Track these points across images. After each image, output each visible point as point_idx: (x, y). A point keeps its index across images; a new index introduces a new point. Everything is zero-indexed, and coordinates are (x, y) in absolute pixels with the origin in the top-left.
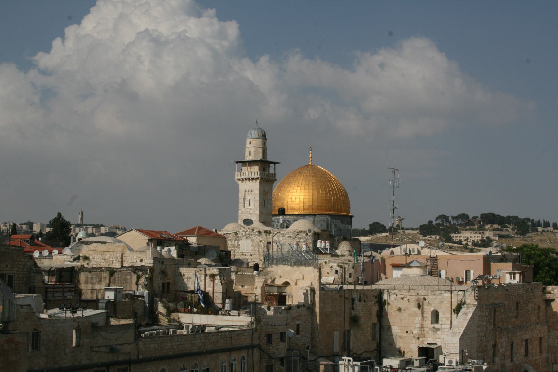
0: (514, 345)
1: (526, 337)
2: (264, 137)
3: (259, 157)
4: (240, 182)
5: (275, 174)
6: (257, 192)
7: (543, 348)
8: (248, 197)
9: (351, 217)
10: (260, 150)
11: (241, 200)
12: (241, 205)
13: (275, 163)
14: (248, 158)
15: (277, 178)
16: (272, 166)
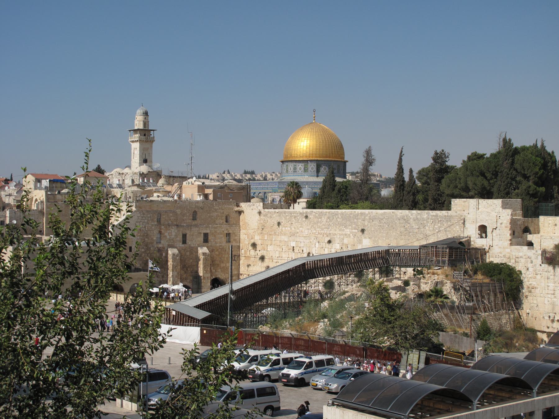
0: (187, 235)
1: (205, 232)
2: (146, 114)
3: (141, 127)
4: (132, 143)
5: (154, 137)
6: (138, 149)
7: (232, 240)
8: (136, 152)
9: (345, 162)
10: (142, 123)
11: (132, 154)
12: (132, 157)
13: (154, 130)
14: (136, 128)
15: (155, 139)
16: (152, 132)
